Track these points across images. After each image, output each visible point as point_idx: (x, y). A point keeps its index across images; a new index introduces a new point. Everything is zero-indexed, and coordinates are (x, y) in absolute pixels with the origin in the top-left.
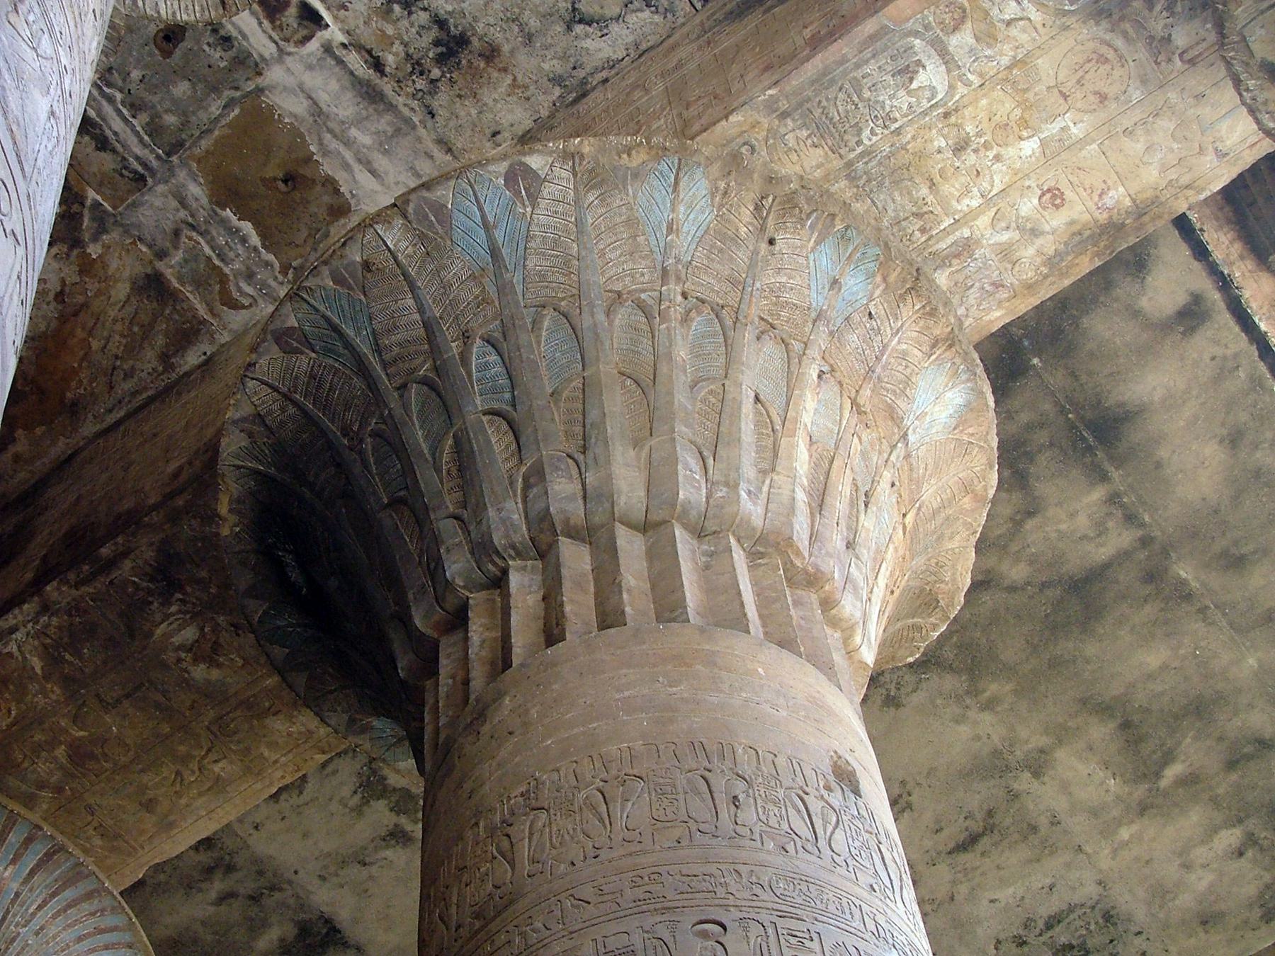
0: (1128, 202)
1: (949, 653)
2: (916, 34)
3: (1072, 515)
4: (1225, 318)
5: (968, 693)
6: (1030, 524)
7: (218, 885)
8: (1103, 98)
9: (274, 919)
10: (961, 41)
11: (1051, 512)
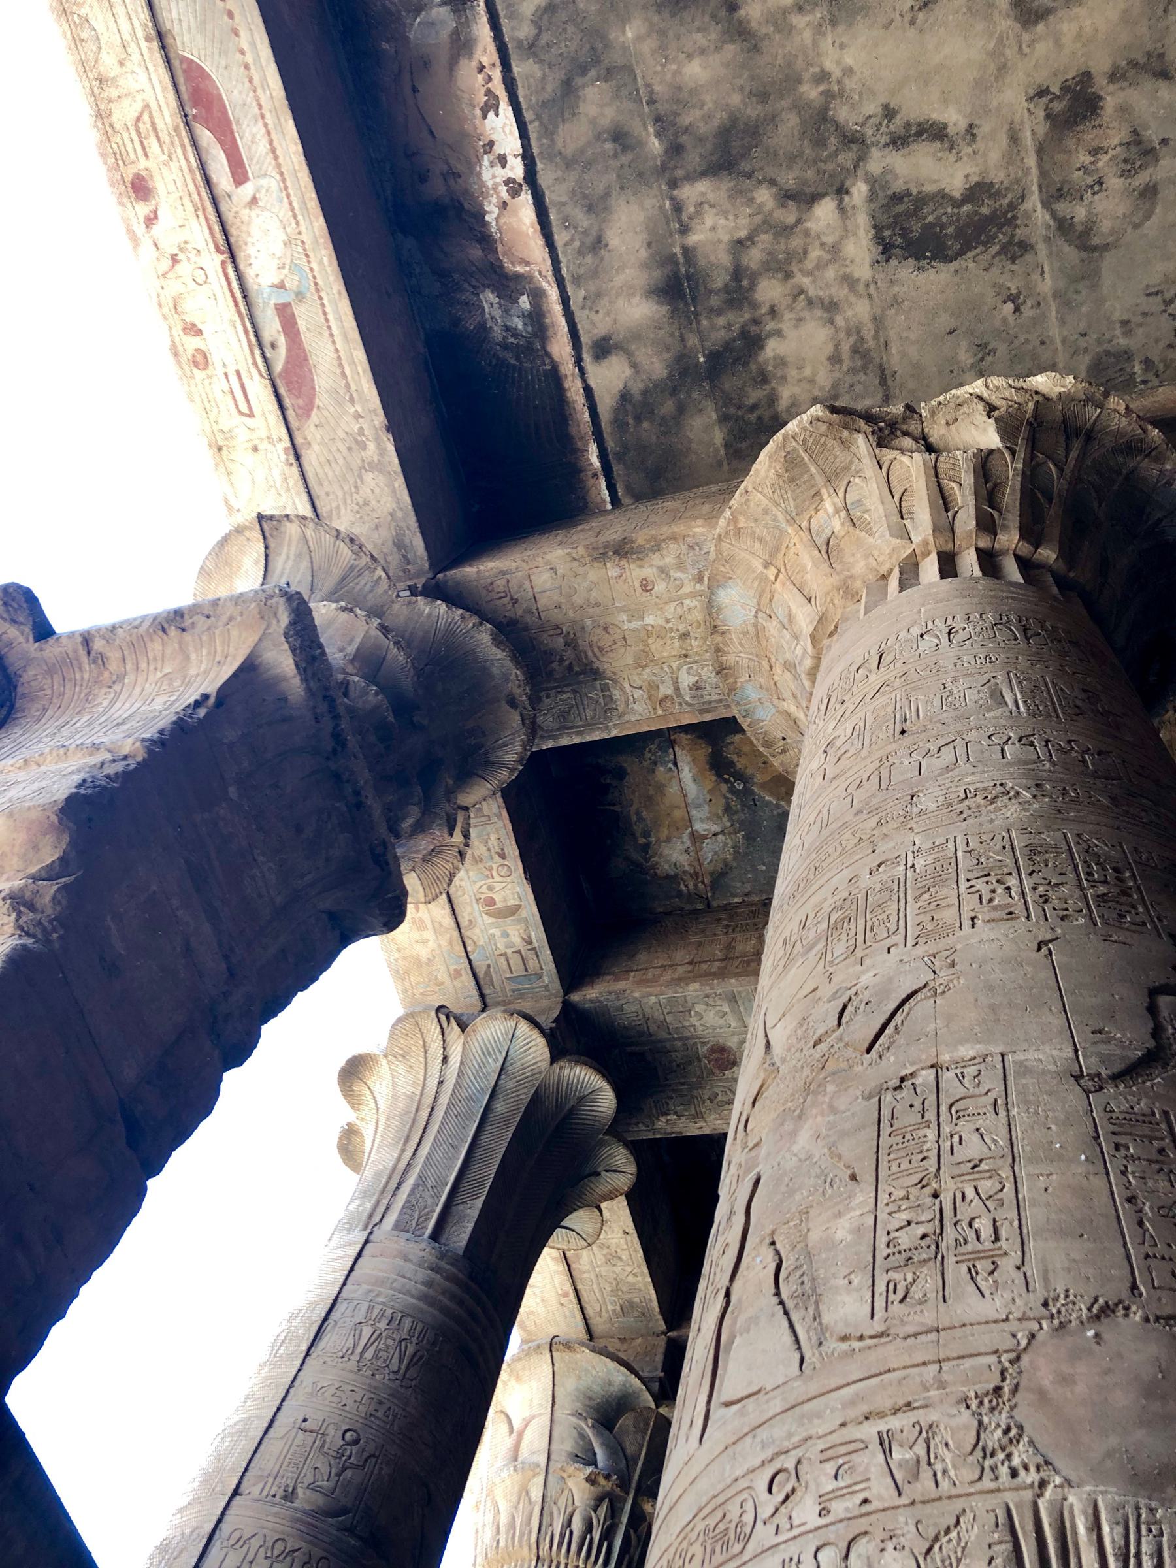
0: (608, 565)
1: (833, 142)
2: (687, 703)
3: (713, 229)
4: (585, 339)
5: (833, 97)
6: (743, 234)
8: (605, 629)
10: (666, 690)
11: (726, 238)
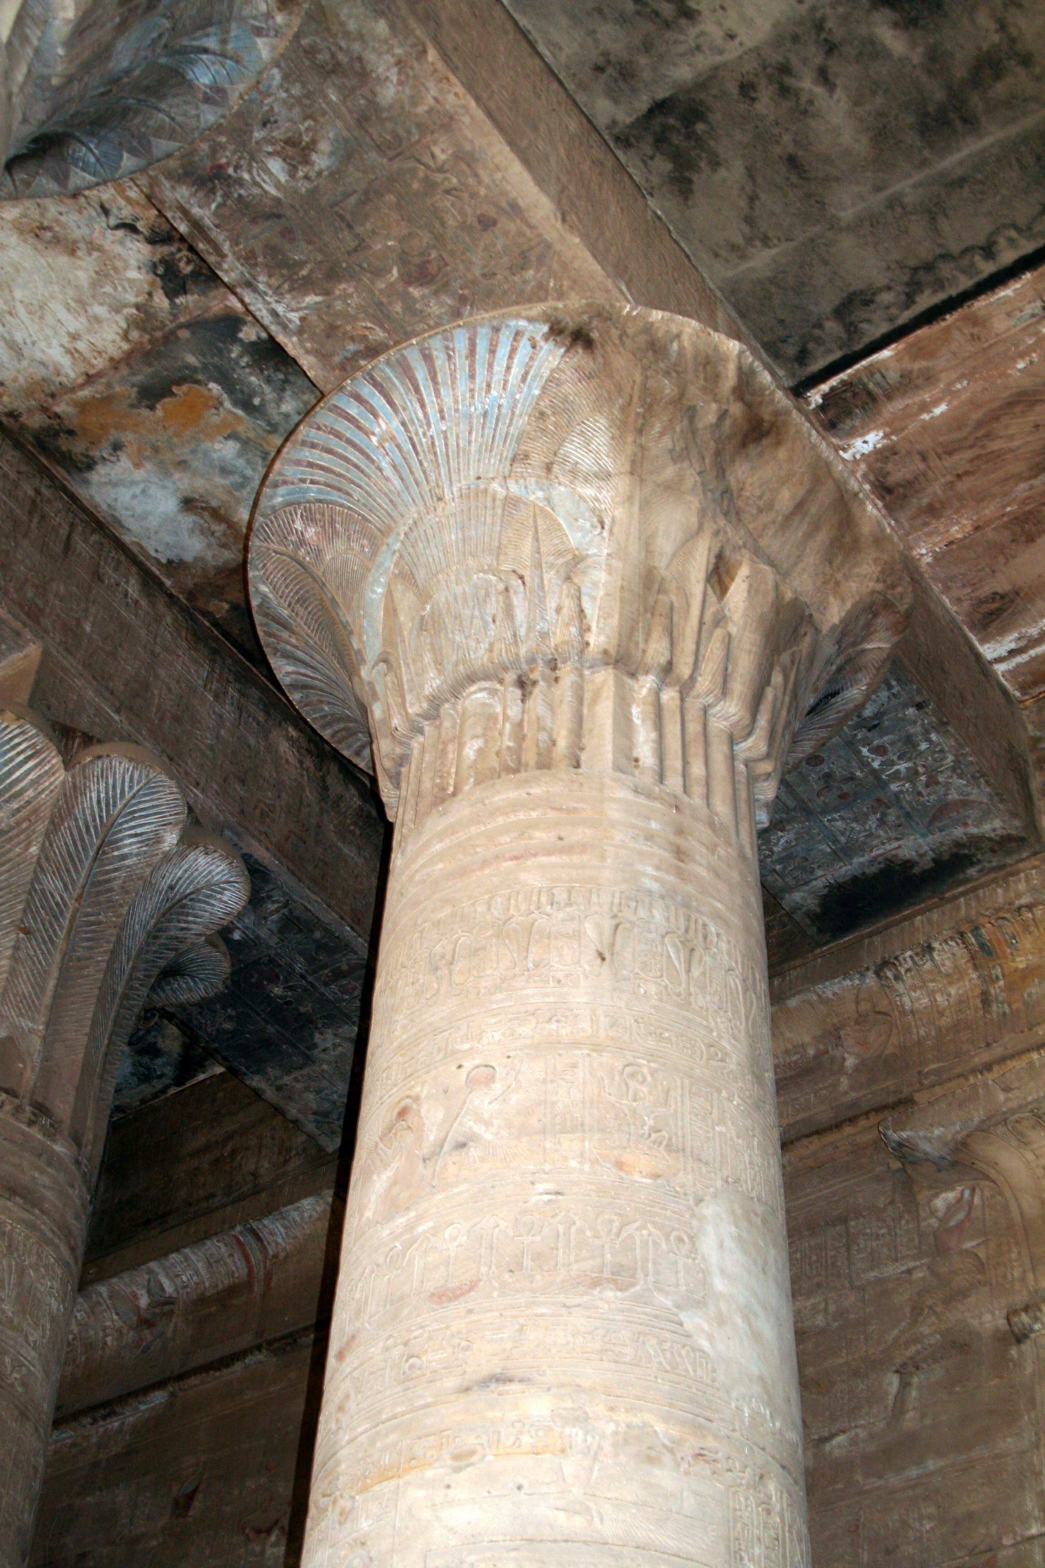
7: (807, 84)
9: (863, 30)
